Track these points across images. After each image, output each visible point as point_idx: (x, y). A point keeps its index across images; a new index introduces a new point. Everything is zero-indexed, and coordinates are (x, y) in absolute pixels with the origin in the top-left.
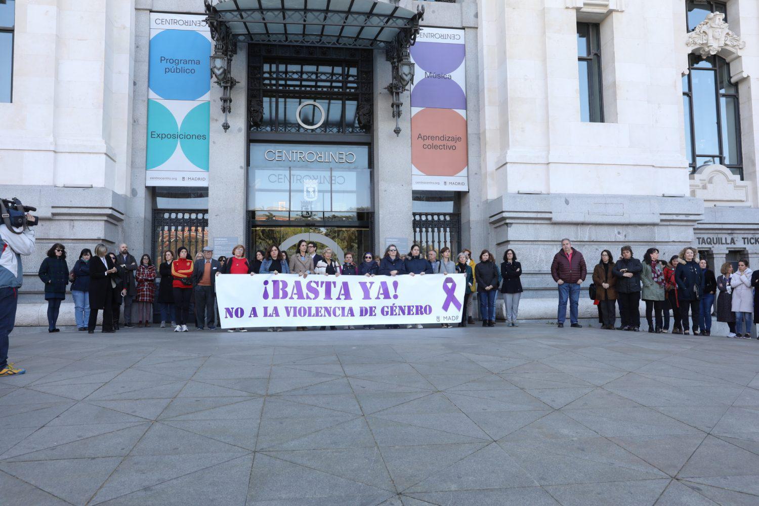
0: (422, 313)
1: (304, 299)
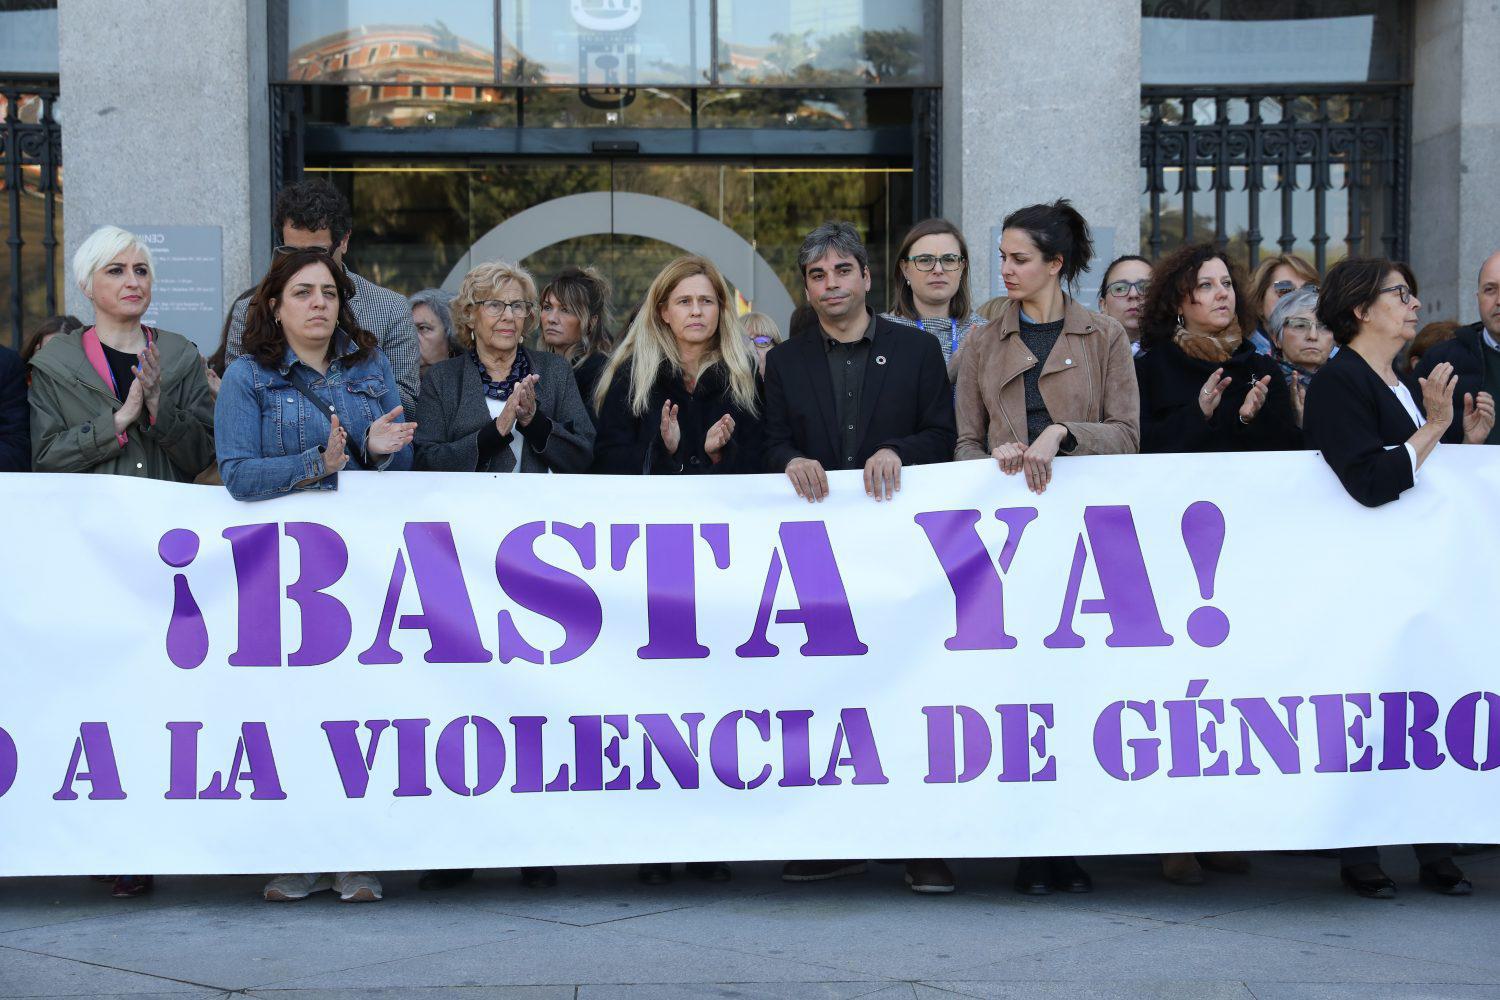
1: (486, 657)
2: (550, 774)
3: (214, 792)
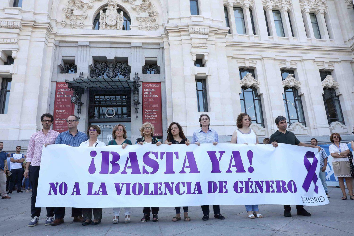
0: (285, 191)
1: (140, 173)
2: (150, 192)
3: (95, 194)
